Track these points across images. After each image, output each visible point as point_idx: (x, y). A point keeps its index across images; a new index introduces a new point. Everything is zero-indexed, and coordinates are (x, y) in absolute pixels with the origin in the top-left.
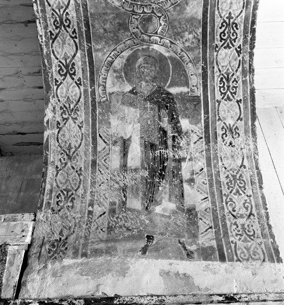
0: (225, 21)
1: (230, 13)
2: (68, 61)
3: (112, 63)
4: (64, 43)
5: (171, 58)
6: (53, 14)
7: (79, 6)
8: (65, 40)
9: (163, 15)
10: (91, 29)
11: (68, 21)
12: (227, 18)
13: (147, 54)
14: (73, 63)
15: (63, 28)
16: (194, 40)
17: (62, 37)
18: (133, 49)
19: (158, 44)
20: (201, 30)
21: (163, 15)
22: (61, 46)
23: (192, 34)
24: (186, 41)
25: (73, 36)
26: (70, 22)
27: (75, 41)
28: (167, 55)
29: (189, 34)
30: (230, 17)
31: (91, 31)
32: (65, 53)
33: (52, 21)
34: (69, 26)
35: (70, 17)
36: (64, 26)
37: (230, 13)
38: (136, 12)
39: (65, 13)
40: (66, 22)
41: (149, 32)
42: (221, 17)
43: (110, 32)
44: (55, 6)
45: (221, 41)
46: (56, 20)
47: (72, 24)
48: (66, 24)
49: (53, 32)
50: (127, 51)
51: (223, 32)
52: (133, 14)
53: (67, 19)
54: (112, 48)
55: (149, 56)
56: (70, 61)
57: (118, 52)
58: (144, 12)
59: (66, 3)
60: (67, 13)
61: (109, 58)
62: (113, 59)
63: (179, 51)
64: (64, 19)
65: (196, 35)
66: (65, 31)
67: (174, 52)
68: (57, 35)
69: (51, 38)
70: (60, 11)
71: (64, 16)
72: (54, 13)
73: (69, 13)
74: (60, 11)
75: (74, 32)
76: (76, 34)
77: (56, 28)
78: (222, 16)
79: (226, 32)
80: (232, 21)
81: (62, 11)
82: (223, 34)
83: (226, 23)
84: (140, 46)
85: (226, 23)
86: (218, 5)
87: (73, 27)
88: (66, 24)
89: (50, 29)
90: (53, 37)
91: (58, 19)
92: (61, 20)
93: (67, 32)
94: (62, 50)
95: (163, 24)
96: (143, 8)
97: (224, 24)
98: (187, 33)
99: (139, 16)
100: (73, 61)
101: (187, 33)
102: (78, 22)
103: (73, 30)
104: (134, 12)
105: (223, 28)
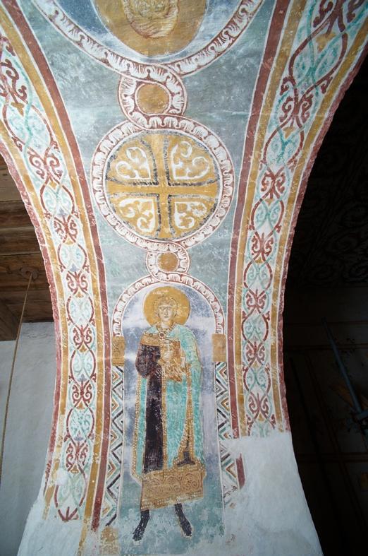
0: (23, 98)
1: (22, 113)
2: (325, 30)
3: (231, 22)
4: (312, 70)
5: (100, 30)
6: (304, 121)
7: (260, 129)
8: (307, 75)
9: (131, 113)
10: (253, 96)
11: (286, 108)
12: (23, 106)
13: (152, 43)
14: (315, 26)
15: (300, 96)
16: (64, 65)
17: (311, 81)
18: (181, 56)
19: (133, 62)
20: (59, 84)
21: (131, 113)
22: (320, 65)
23: (71, 77)
24: (79, 65)
25: (289, 84)
26: (284, 106)
27: (291, 72)
28: (110, 37)
29: (77, 78)
30: (19, 106)
31: (255, 89)
32: (320, 50)
33: (311, 110)
34: (289, 99)
35: (282, 114)
36: (296, 99)
37: (22, 113)
38: (173, 117)
39: (284, 121)
40: (290, 107)
41: (152, 87)
42: (33, 106)
43: (222, 87)
44: (294, 132)
45: (6, 60)
46: (304, 110)
47: (282, 103)
48: (292, 103)
49: (320, 91)
50: (195, 51)
51: (15, 79)
52: (180, 114)
53: (286, 111)
54: (222, 59)
55: (147, 36)
56: (321, 28)
57: (213, 48)
58: (163, 118)
59: (277, 134)
60: (281, 121)
61: (234, 33)
62: (227, 33)
63: (84, 41)
64: (289, 114)
65: (63, 74)
66: (300, 89)
67: (95, 42)
68: (315, 86)
69: (329, 82)
70: (292, 123)
71: (288, 118)
72: (301, 123)
73: (279, 120)
74: (292, 123)
75: (284, 89)
76: (282, 87)
77: (311, 96)
78: (32, 109)
79: (10, 80)
80: (12, 100)
81: (288, 125)
82: (13, 74)
83: (18, 96)
84: (168, 60)
85: (18, 96)
86: (48, 126)
87: (282, 99)
88: (292, 103)
89: (322, 96)
90: (325, 82)
91: (301, 110)
92: (296, 111)
93: (295, 91)
94: (323, 56)
95: (129, 99)
96: (163, 124)
97: (22, 95)
98: (82, 79)
99: (170, 111)
100: (313, 30)
101: (82, 79)
102: (271, 106)
103: (285, 93)
104: (178, 118)
105: (19, 86)
